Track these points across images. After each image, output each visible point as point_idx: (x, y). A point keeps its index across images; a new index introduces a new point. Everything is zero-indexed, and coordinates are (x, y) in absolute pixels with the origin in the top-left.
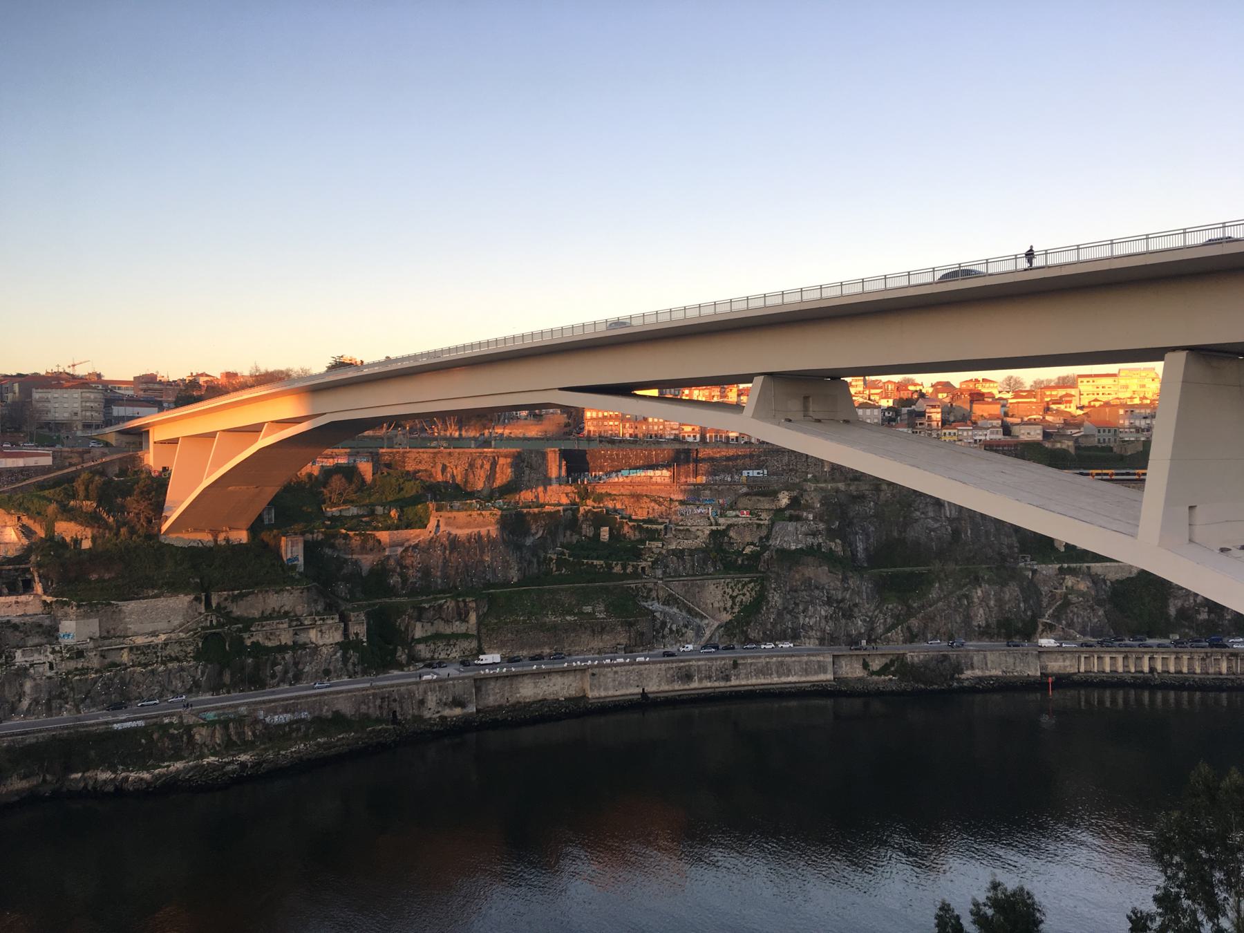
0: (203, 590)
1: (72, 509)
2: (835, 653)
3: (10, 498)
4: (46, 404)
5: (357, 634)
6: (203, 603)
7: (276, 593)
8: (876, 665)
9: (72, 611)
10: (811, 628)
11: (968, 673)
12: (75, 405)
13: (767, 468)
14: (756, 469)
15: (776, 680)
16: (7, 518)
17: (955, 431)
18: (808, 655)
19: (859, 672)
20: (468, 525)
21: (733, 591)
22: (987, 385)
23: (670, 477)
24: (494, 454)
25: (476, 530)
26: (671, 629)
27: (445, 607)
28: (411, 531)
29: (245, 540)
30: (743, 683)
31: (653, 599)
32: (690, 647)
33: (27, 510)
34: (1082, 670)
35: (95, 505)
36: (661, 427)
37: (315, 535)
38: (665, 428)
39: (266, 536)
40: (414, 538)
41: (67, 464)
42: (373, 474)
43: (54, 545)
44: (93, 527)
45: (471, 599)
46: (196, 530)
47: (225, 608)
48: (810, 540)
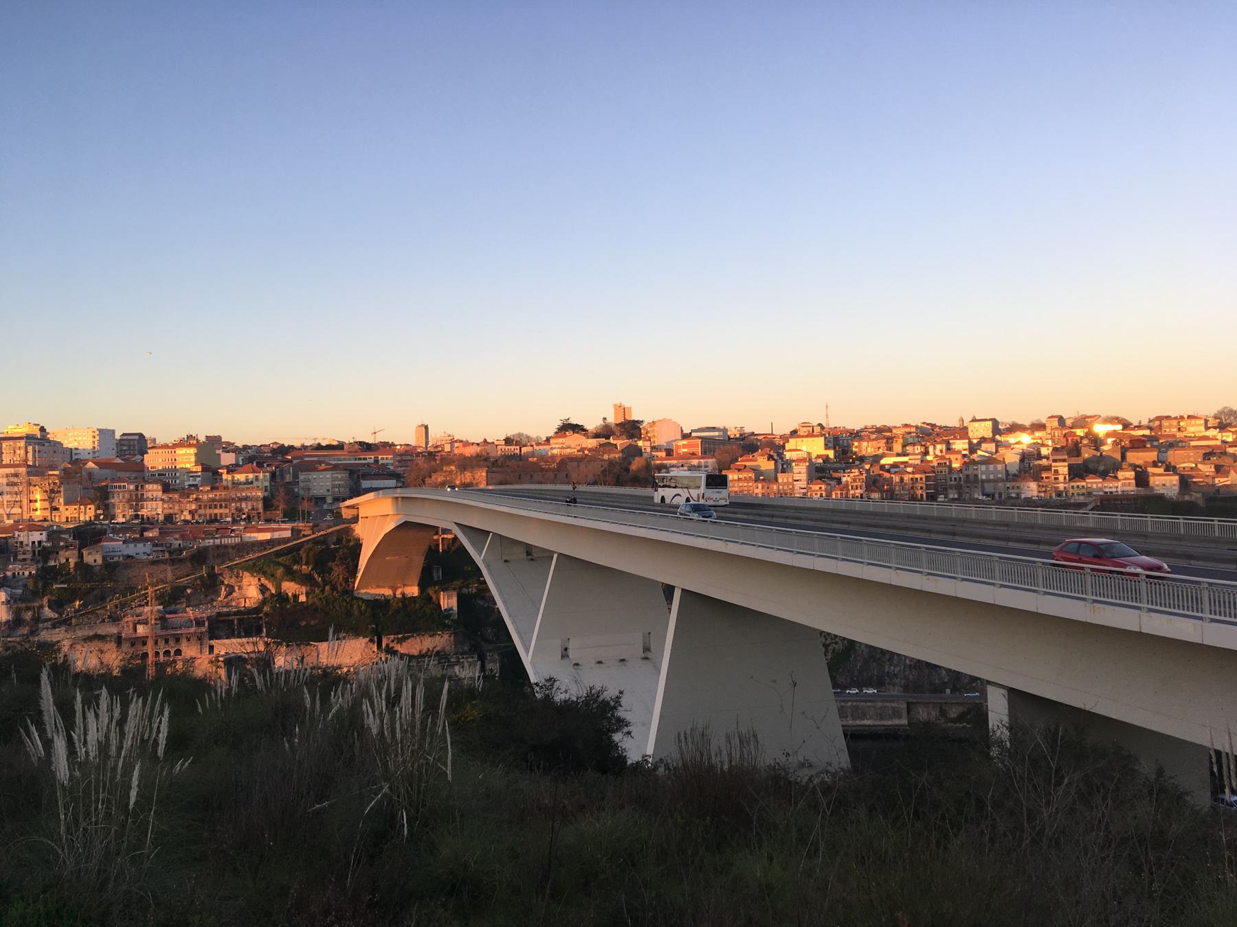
0: (376, 636)
1: (295, 572)
2: (911, 700)
3: (254, 564)
4: (308, 483)
5: (491, 670)
6: (376, 644)
7: (430, 636)
8: (953, 713)
9: (283, 649)
10: (896, 676)
12: (328, 484)
16: (251, 579)
17: (1084, 484)
18: (882, 701)
21: (826, 639)
22: (1193, 422)
29: (416, 594)
33: (265, 573)
35: (310, 568)
36: (791, 487)
37: (470, 590)
38: (793, 487)
39: (430, 591)
41: (301, 535)
43: (281, 597)
44: (306, 586)
46: (378, 587)
47: (393, 647)
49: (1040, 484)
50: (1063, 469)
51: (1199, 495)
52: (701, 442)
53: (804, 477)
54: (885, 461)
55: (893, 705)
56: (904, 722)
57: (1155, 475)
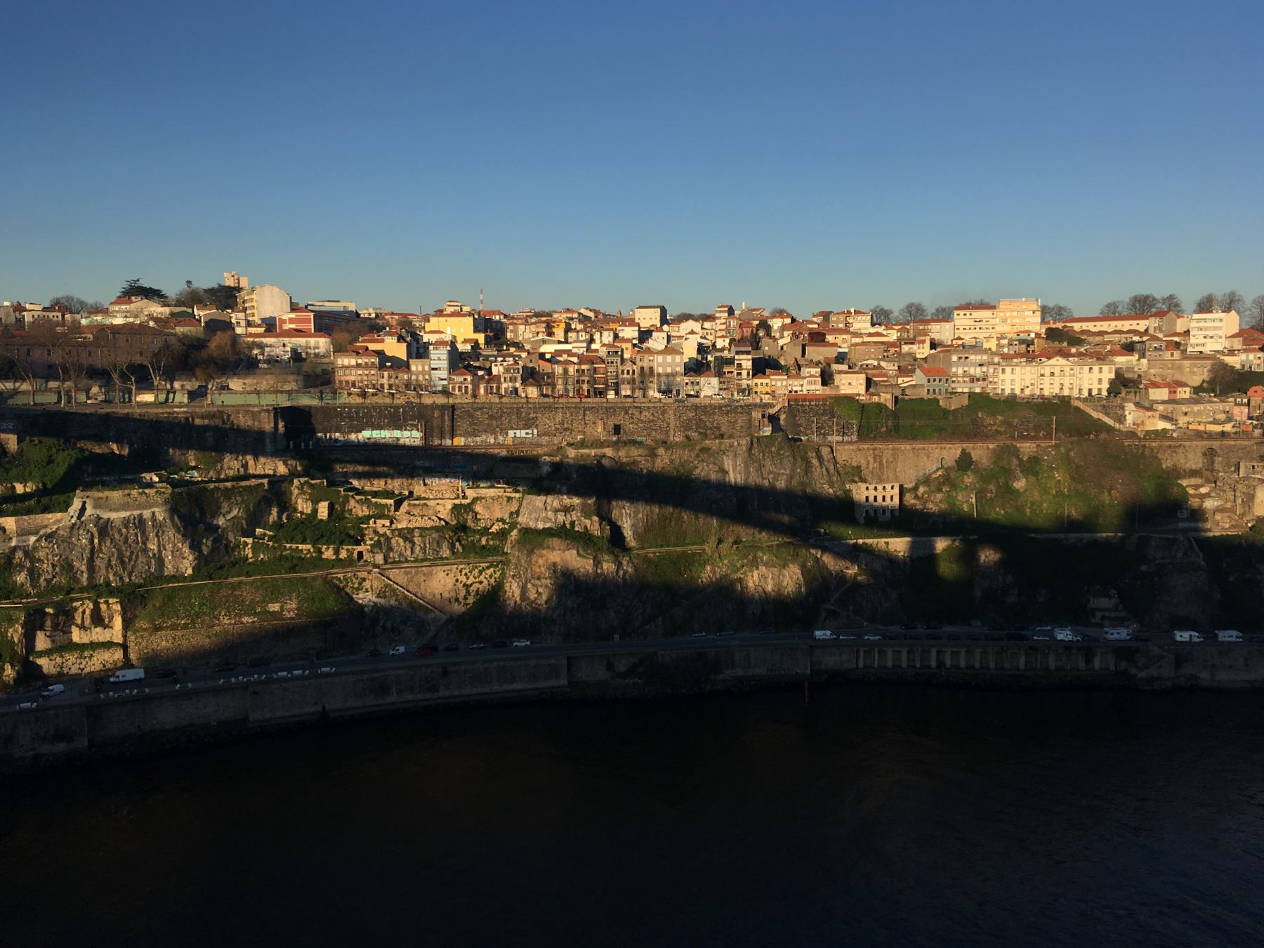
8: (622, 666)
11: (729, 673)
13: (537, 427)
14: (524, 428)
15: (496, 688)
19: (602, 674)
20: (125, 507)
21: (468, 578)
23: (421, 438)
24: (188, 415)
25: (136, 513)
26: (384, 627)
27: (81, 610)
28: (50, 516)
30: (455, 693)
31: (367, 591)
32: (402, 649)
34: (861, 664)
36: (427, 377)
40: (54, 523)
42: (18, 443)
45: (115, 600)
48: (561, 517)
49: (722, 380)
50: (747, 364)
51: (889, 396)
52: (314, 316)
53: (444, 364)
54: (548, 349)
55: (553, 661)
56: (563, 681)
57: (840, 372)
